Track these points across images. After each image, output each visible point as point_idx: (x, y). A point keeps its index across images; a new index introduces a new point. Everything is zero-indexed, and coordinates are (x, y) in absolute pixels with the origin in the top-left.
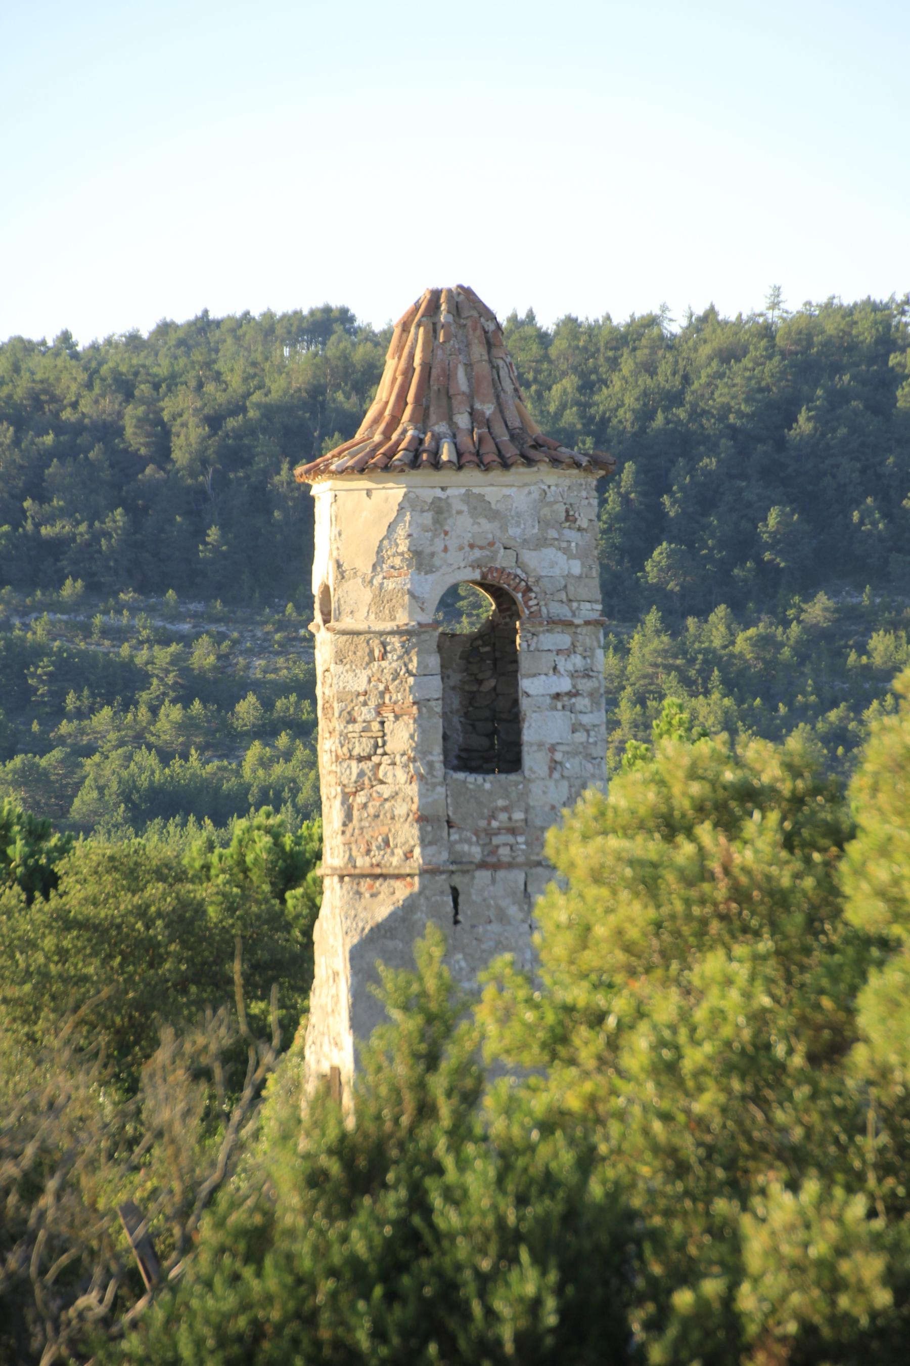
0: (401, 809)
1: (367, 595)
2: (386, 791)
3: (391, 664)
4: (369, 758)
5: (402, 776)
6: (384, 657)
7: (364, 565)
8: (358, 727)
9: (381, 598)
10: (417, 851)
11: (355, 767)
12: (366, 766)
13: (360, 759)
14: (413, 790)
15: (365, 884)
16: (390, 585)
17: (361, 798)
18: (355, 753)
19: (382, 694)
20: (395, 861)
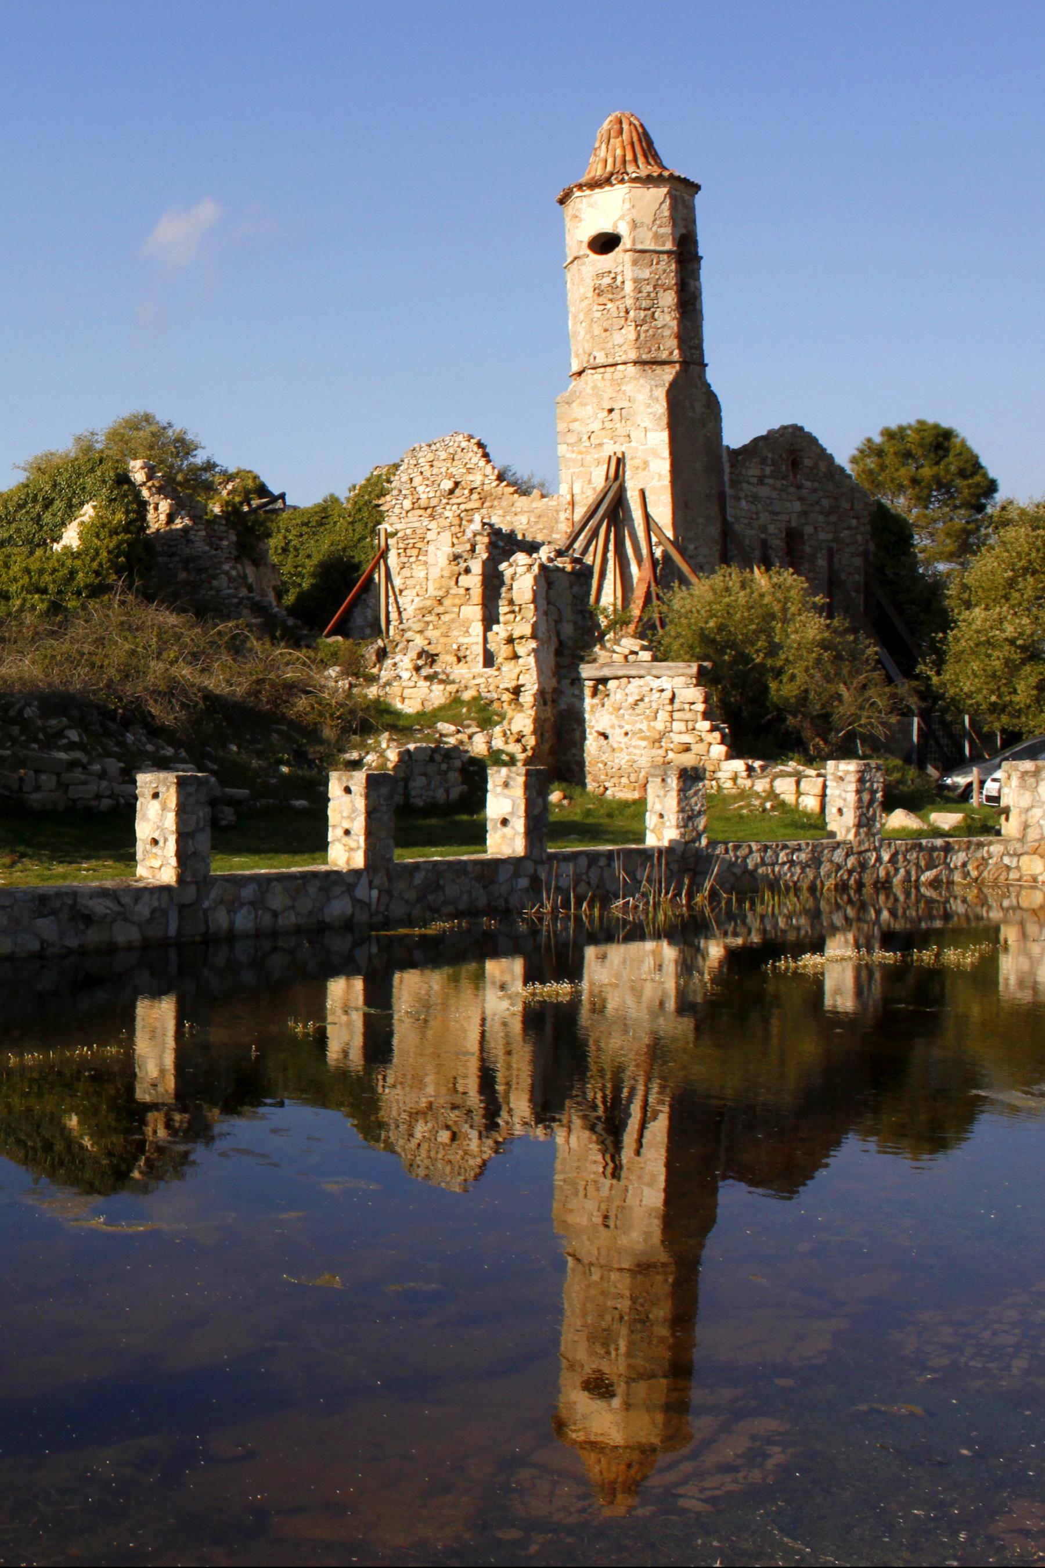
0: (667, 332)
1: (650, 234)
2: (659, 324)
3: (663, 265)
4: (649, 309)
5: (668, 318)
6: (658, 263)
7: (648, 221)
8: (644, 294)
9: (656, 236)
10: (676, 352)
11: (642, 314)
12: (649, 312)
13: (645, 310)
14: (674, 323)
15: (647, 367)
16: (662, 230)
17: (644, 328)
18: (643, 306)
19: (658, 280)
20: (664, 356)
